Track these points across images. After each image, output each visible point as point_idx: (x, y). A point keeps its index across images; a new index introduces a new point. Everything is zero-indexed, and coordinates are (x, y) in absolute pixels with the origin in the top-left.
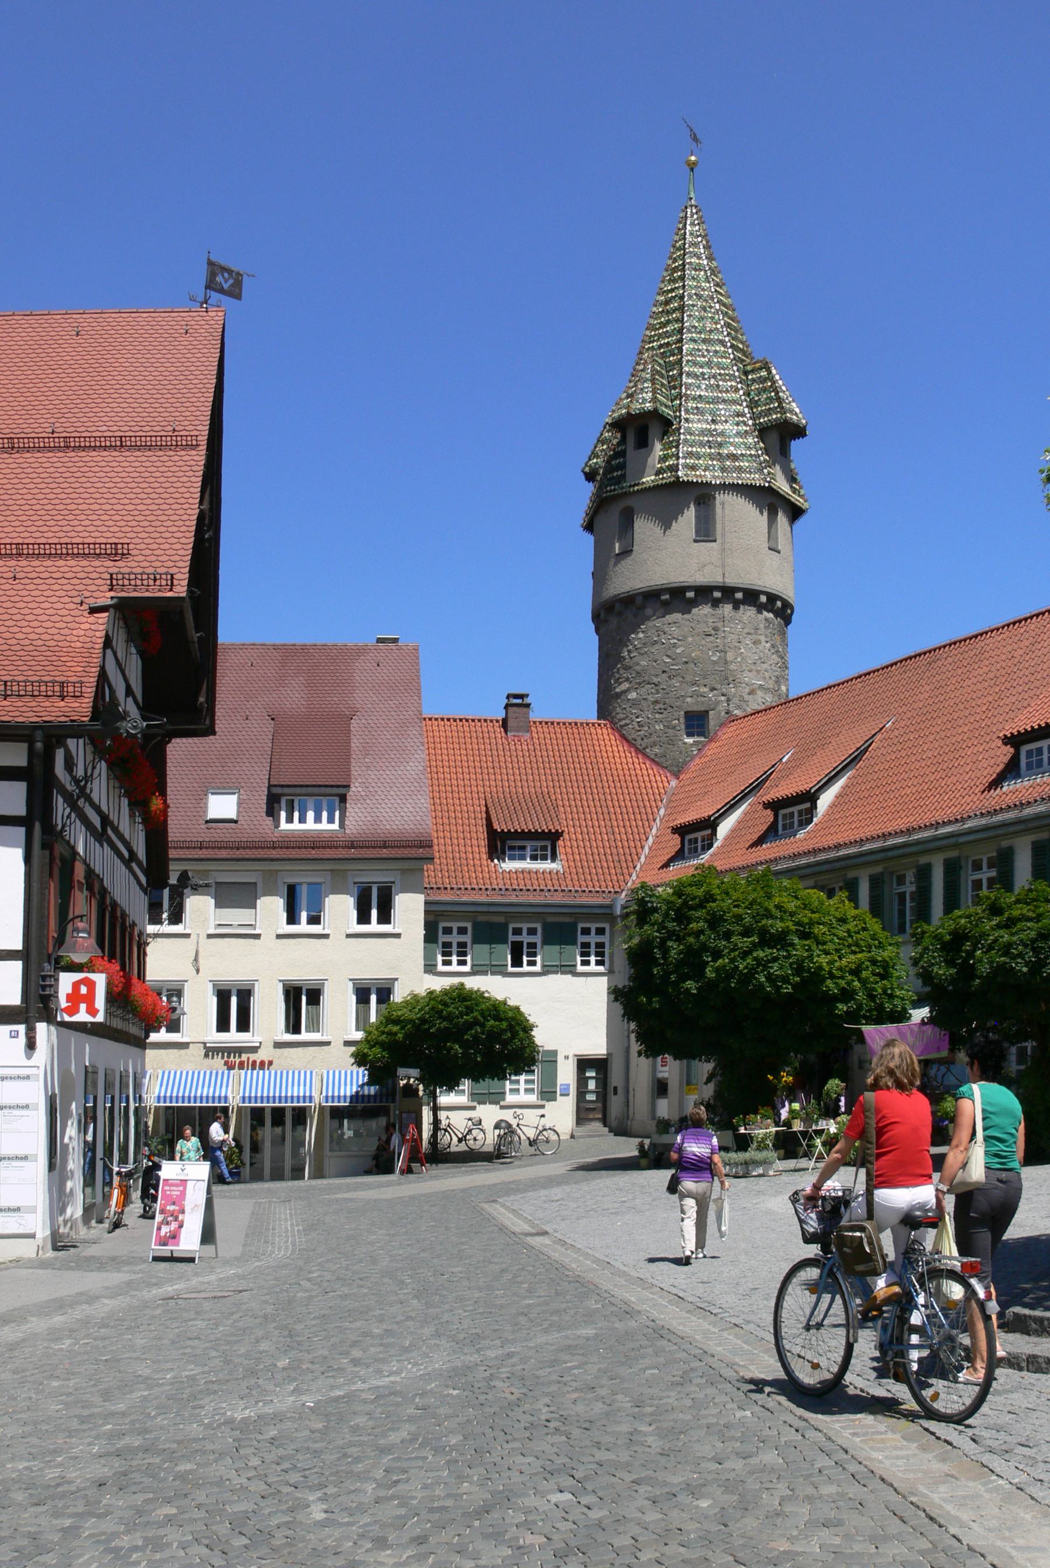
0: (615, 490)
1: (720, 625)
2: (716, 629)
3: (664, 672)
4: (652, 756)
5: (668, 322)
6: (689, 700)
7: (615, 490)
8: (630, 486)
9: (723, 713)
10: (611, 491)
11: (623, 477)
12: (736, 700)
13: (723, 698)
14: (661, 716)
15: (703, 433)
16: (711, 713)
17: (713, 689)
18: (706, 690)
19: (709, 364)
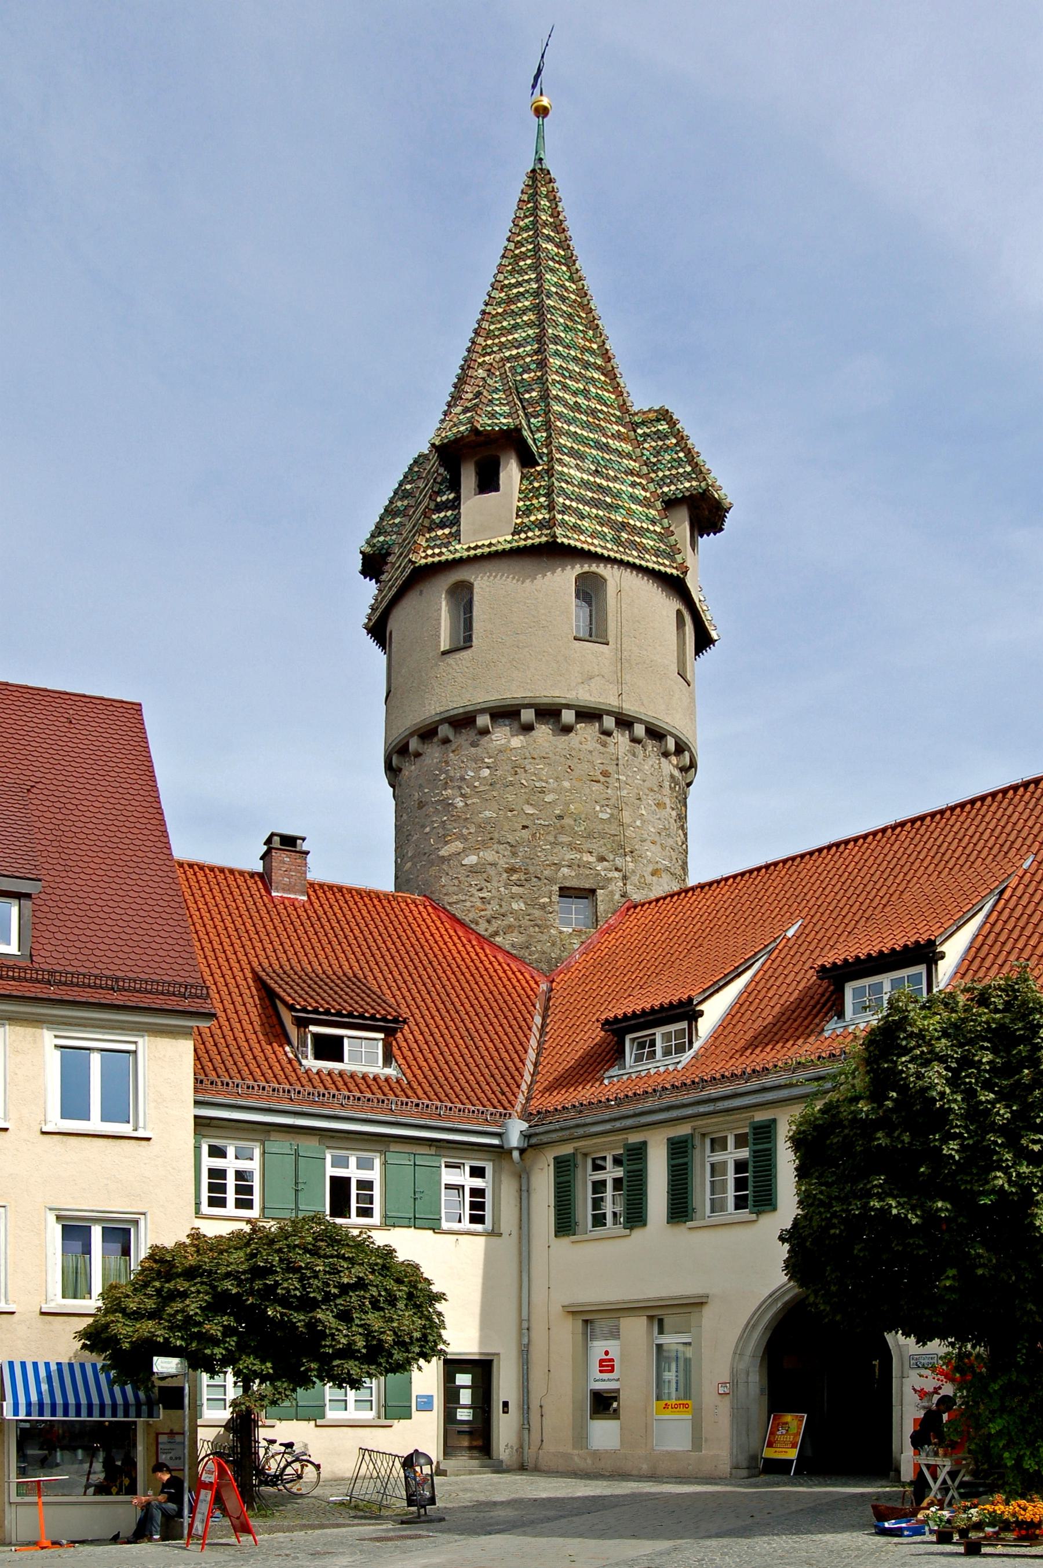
0: (441, 554)
1: (612, 769)
2: (605, 774)
3: (524, 827)
4: (508, 947)
5: (515, 327)
6: (565, 870)
7: (441, 554)
8: (469, 549)
9: (617, 897)
10: (433, 555)
11: (456, 536)
12: (635, 879)
13: (616, 874)
14: (520, 890)
15: (584, 484)
16: (599, 892)
17: (602, 859)
18: (592, 859)
19: (585, 393)
